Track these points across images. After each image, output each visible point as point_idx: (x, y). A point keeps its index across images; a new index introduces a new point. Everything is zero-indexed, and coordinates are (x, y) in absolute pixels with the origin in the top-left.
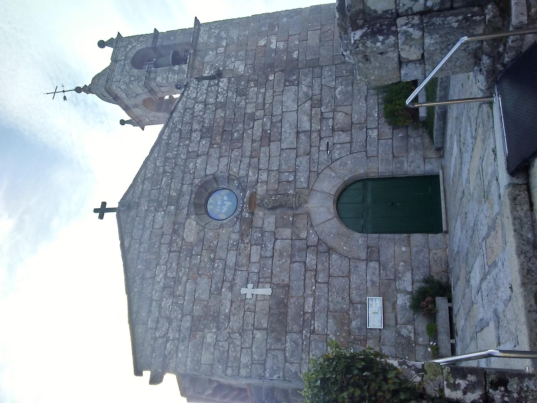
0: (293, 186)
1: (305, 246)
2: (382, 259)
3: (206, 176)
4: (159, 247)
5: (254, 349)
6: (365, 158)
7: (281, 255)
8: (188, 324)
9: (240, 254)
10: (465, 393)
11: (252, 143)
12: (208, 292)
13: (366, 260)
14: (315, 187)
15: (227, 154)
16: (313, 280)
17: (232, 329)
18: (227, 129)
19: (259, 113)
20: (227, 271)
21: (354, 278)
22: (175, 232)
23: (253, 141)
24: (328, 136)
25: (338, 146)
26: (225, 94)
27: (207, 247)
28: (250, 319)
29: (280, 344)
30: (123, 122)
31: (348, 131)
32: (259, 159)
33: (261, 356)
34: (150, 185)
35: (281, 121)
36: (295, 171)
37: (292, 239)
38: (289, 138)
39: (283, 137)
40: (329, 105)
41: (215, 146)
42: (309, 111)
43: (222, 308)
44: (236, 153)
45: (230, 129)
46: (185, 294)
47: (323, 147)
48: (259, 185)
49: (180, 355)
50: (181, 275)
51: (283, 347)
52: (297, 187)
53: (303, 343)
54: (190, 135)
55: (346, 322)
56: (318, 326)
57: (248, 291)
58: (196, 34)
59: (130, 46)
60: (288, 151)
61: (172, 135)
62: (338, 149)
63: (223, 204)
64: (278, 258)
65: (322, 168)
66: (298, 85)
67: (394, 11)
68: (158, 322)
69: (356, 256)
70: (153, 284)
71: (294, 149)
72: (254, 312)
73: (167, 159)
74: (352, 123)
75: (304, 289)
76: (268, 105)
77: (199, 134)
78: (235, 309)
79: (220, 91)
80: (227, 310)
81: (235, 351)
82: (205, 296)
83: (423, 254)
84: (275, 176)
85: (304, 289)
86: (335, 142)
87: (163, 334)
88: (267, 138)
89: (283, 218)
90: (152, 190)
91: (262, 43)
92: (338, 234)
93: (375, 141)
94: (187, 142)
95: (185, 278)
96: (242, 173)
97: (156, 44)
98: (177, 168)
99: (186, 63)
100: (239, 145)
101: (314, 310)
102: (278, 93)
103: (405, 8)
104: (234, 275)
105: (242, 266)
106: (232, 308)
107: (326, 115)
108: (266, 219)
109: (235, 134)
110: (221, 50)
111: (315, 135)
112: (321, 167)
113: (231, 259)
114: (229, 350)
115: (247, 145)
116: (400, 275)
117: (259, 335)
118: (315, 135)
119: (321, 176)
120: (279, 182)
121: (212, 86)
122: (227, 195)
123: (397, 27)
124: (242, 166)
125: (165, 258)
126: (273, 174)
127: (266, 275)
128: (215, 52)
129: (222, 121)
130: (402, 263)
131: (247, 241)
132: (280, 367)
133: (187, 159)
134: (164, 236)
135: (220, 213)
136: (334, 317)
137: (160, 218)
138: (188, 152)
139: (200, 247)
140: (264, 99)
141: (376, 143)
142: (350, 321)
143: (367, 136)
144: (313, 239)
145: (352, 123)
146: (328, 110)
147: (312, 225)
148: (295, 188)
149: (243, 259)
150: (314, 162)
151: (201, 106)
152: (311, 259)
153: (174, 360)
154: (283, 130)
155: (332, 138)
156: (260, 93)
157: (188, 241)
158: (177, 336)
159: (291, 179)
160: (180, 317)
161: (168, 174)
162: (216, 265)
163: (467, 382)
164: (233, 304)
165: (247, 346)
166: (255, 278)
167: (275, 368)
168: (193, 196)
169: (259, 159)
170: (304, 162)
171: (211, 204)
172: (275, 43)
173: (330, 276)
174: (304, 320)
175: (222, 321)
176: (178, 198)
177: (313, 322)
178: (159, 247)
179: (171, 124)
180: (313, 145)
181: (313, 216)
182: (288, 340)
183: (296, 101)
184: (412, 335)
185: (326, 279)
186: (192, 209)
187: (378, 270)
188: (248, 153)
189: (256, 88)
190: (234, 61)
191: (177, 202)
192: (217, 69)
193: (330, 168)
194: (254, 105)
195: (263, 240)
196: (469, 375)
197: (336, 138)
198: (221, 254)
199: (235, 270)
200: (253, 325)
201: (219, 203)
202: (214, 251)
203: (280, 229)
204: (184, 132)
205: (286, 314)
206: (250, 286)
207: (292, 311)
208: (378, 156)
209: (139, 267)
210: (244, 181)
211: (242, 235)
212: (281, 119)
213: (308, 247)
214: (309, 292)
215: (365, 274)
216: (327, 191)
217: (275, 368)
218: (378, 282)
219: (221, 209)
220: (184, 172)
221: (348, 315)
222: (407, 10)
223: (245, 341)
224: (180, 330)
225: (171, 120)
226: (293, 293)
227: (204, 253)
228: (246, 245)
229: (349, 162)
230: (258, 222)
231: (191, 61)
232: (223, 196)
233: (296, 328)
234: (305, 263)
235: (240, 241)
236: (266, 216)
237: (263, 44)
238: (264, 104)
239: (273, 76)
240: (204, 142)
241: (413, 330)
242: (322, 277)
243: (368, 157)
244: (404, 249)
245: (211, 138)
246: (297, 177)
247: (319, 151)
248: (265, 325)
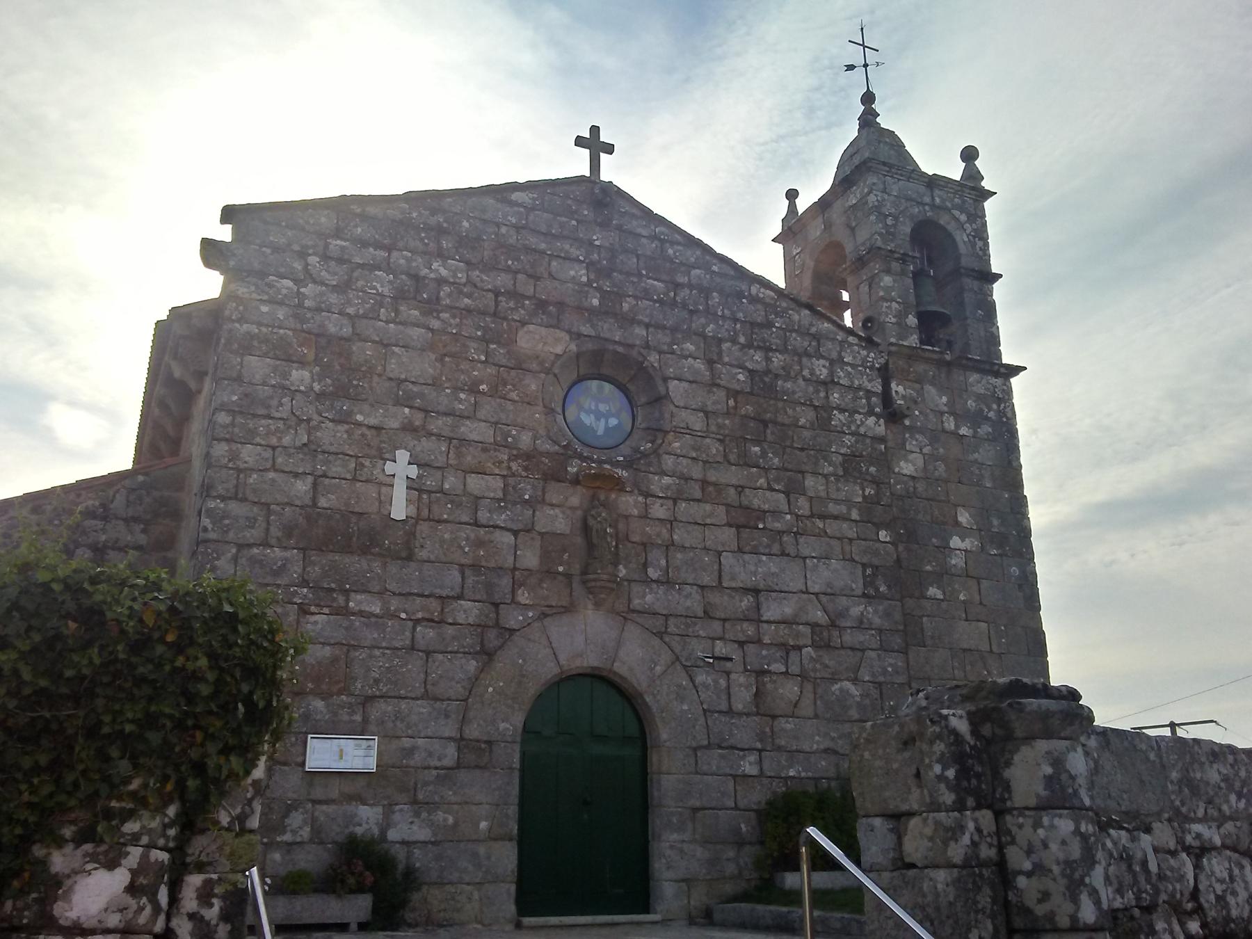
0: (636, 577)
1: (497, 598)
2: (463, 775)
3: (665, 379)
4: (508, 270)
5: (271, 475)
6: (694, 744)
7: (480, 543)
8: (332, 329)
9: (485, 450)
10: (192, 916)
11: (736, 487)
12: (403, 377)
13: (462, 739)
14: (630, 627)
15: (713, 428)
16: (420, 615)
17: (317, 428)
18: (769, 431)
19: (803, 506)
20: (449, 420)
21: (423, 708)
22: (541, 305)
23: (740, 489)
24: (748, 660)
25: (723, 682)
26: (849, 428)
27: (505, 376)
28: (339, 469)
29: (280, 534)
30: (792, 195)
31: (757, 706)
32: (699, 501)
33: (254, 491)
34: (649, 253)
35: (784, 554)
37: (515, 569)
38: (742, 570)
39: (747, 557)
40: (818, 666)
41: (731, 402)
42: (804, 619)
43: (366, 407)
44: (715, 448)
45: (770, 437)
46: (400, 323)
47: (721, 648)
48: (640, 499)
49: (265, 309)
50: (444, 315)
51: (273, 542)
52: (633, 584)
53: (278, 586)
54: (759, 348)
55: (324, 687)
56: (316, 623)
57: (401, 467)
58: (987, 367)
59: (963, 218)
60: (716, 567)
61: (759, 306)
62: (716, 682)
63: (599, 415)
64: (472, 536)
65: (674, 644)
66: (864, 595)
67: (1009, 804)
68: (341, 261)
69: (471, 714)
70: (425, 253)
71: (720, 582)
72: (355, 479)
73: (705, 292)
74: (774, 717)
75: (400, 594)
76: (821, 526)
77: (761, 367)
78: (363, 435)
79: (857, 417)
80: (359, 418)
81: (269, 433)
82: (393, 368)
83: (471, 868)
84: (658, 535)
85: (400, 594)
86: (733, 676)
87: (313, 272)
88: (745, 520)
89: (565, 551)
90: (638, 256)
91: (964, 518)
92: (523, 676)
93: (732, 767)
94: (742, 340)
95: (435, 324)
96: (669, 462)
97: (968, 276)
98: (685, 314)
99: (922, 342)
100: (732, 458)
101: (353, 614)
102: (847, 548)
103: (1014, 830)
104: (439, 436)
105: (459, 455)
106: (364, 429)
107: (794, 656)
108: (563, 513)
109: (757, 449)
110: (950, 424)
111: (750, 630)
113: (476, 431)
114: (272, 418)
115: (732, 476)
116: (424, 815)
117: (302, 487)
118: (750, 630)
119: (656, 642)
120: (644, 545)
121: (868, 399)
122: (618, 426)
123: (974, 809)
124: (684, 461)
125: (482, 281)
126: (665, 531)
127: (435, 508)
128: (946, 409)
129: (787, 421)
130: (451, 820)
132: (226, 532)
133: (705, 337)
134: (532, 281)
135: (580, 408)
136: (335, 660)
137: (572, 273)
138: (720, 341)
139: (504, 362)
140: (836, 518)
141: (728, 771)
142: (325, 696)
143: (742, 750)
144: (514, 618)
145: (774, 717)
146: (805, 662)
147: (545, 615)
148: (629, 581)
149: (474, 457)
150: (688, 626)
151: (823, 373)
152: (468, 612)
153: (254, 296)
154: (764, 558)
155: (741, 669)
156: (849, 509)
157: (521, 333)
158: (307, 303)
159: (650, 571)
160: (351, 310)
161: (672, 294)
162: (462, 396)
163: (214, 922)
164: (374, 432)
165: (280, 460)
166: (430, 483)
167: (227, 522)
168: (620, 349)
169: (699, 501)
170: (688, 603)
171: (600, 389)
172: (962, 545)
173: (428, 653)
174: (331, 590)
175: (338, 404)
177: (326, 610)
178: (508, 270)
179: (784, 305)
180: (727, 625)
182: (288, 554)
183: (829, 590)
184: (287, 837)
185: (421, 644)
186: (590, 346)
187: (438, 764)
188: (712, 476)
189: (860, 500)
190: (926, 450)
191: (606, 313)
192: (906, 412)
193: (673, 663)
194: (823, 494)
195: (515, 503)
196: (229, 927)
197: (742, 680)
198: (488, 409)
199: (451, 439)
200: (325, 476)
201: (603, 407)
202: (494, 392)
203: (538, 543)
204: (765, 334)
205: (347, 549)
206: (413, 471)
207: (354, 564)
208: (697, 773)
209: (466, 224)
210: (650, 464)
211: (528, 456)
212: (788, 555)
213: (496, 605)
214: (394, 604)
215: (430, 734)
216: (621, 654)
217: (227, 522)
218: (412, 763)
219: (588, 412)
220: (674, 330)
221: (340, 693)
222: (1009, 832)
223: (290, 455)
224: (319, 310)
225: (793, 305)
226: (393, 568)
227: (491, 370)
228: (505, 464)
229: (685, 707)
230: (555, 493)
231: (927, 355)
232: (617, 415)
233: (315, 572)
234: (460, 597)
235: (515, 452)
236: (568, 512)
237: (960, 519)
238: (823, 517)
239: (888, 539)
240: (741, 377)
241: (299, 840)
242: (426, 634)
243: (695, 750)
244: (483, 825)
245: (751, 393)
246: (654, 586)
247: (713, 639)
248: (323, 502)
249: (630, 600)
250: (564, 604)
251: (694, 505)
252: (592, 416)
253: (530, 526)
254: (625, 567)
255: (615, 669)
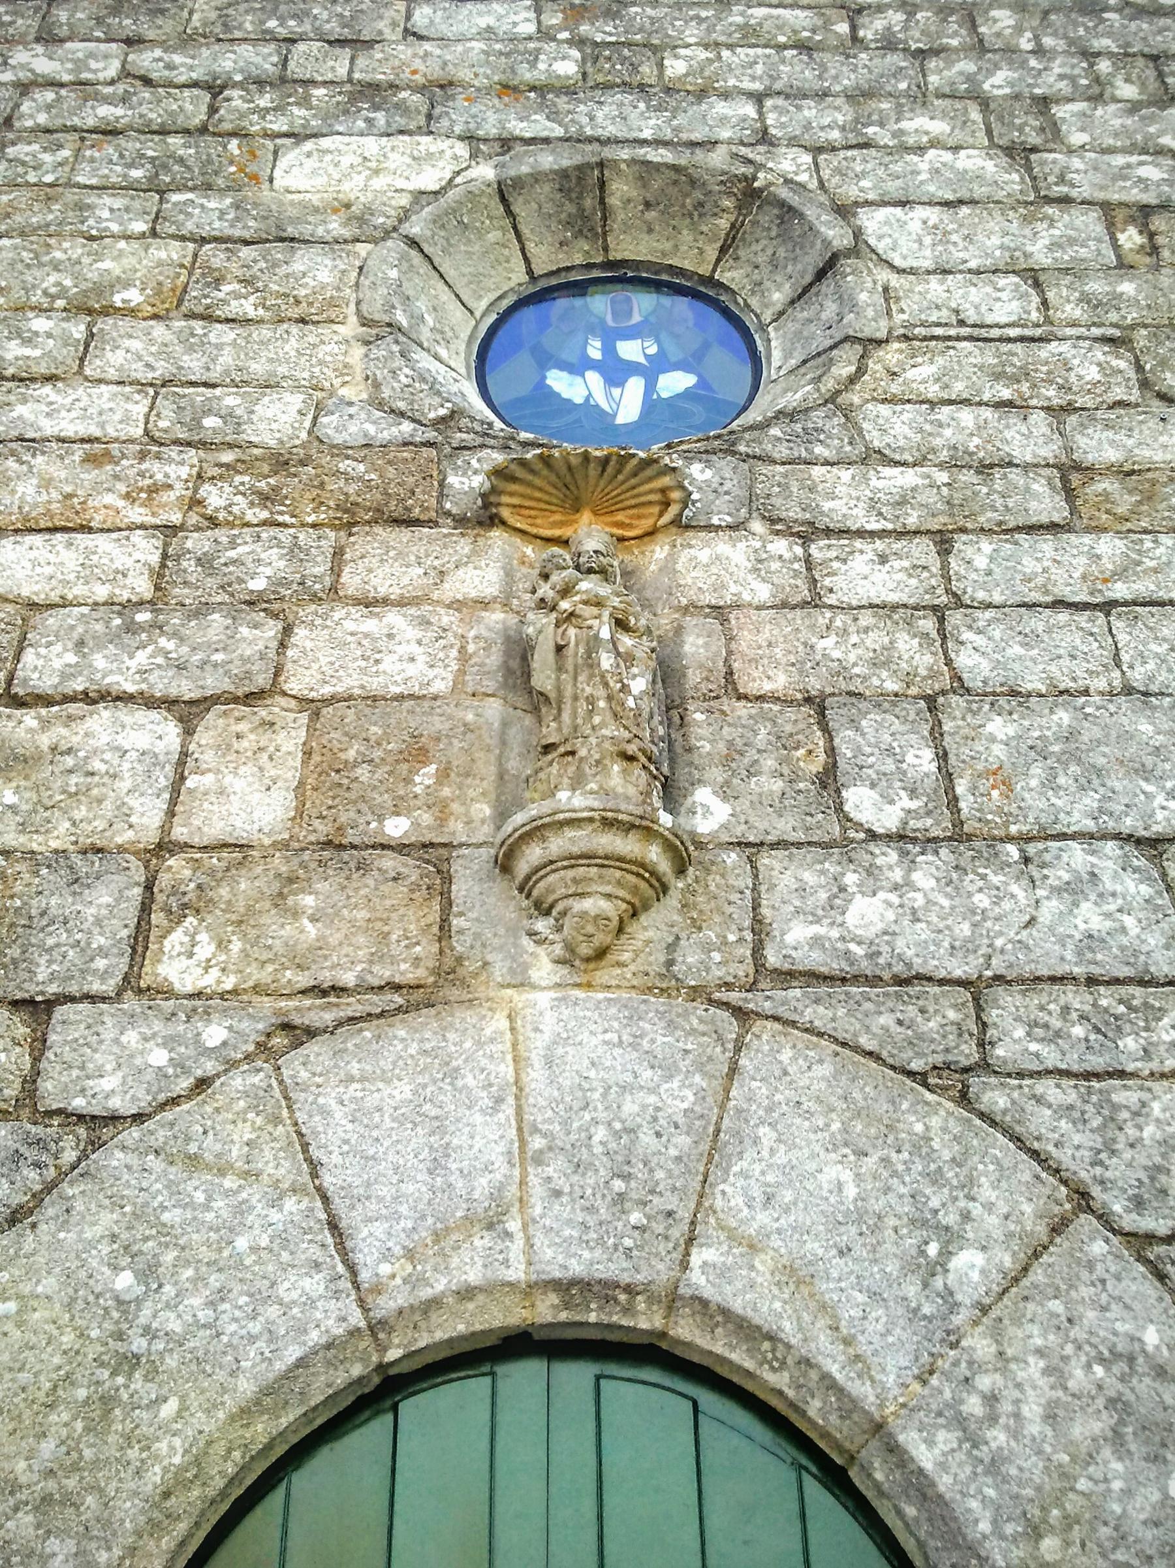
0: (785, 826)
4: (268, 37)
32: (1053, 528)
36: (959, 836)
48: (780, 546)
63: (616, 372)
65: (1041, 1123)
89: (418, 754)
92: (132, 1362)
112: (1050, 1114)
119: (937, 1120)
120: (817, 704)
125: (170, 67)
131: (215, 497)
148: (752, 848)
150: (1107, 1028)
159: (860, 801)
168: (662, 155)
169: (1053, 528)
170: (1089, 917)
176: (642, 88)
178: (268, 37)
181: (405, 1039)
188: (1099, 445)
193: (1058, 1228)
195: (202, 610)
201: (630, 350)
210: (811, 436)
216: (732, 1195)
219: (578, 367)
230: (384, 563)
236: (447, 618)
249: (759, 929)
250: (405, 972)
251: (1047, 545)
252: (593, 377)
253: (262, 680)
254: (725, 792)
255: (698, 1280)
